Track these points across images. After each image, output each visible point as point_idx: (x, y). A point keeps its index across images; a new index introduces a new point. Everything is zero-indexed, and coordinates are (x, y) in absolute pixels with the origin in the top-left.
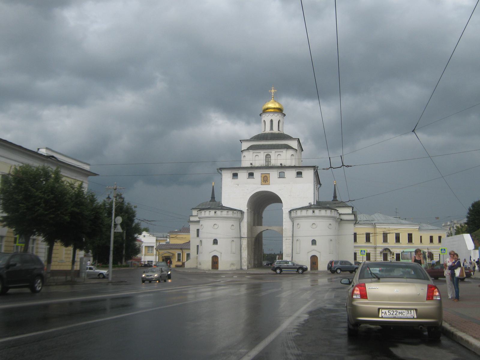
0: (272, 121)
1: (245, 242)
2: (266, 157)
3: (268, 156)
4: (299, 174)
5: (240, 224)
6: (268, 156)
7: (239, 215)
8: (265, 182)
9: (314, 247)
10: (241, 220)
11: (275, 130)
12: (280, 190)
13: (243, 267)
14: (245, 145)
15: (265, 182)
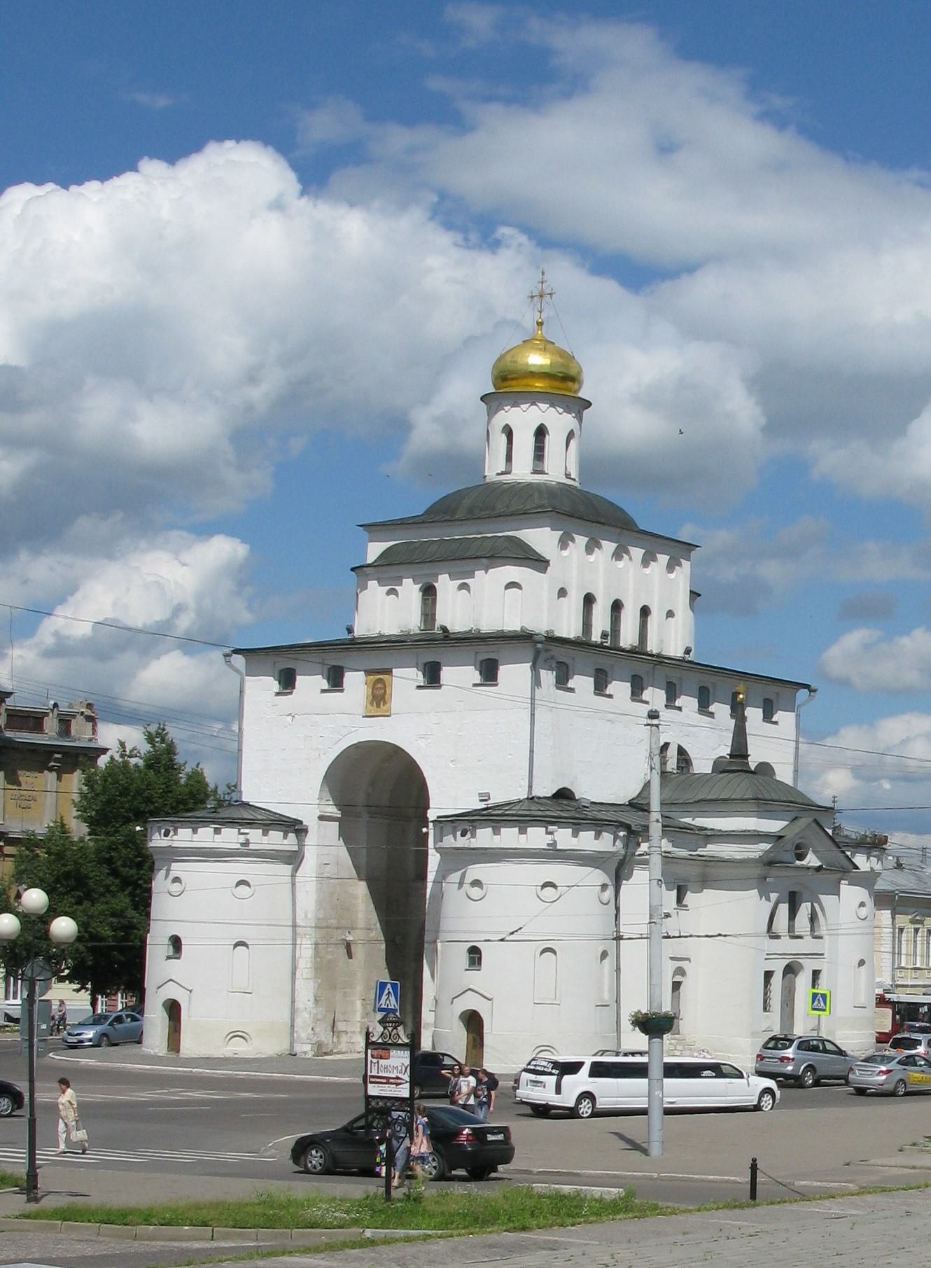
0: (509, 432)
1: (306, 953)
2: (424, 601)
3: (429, 592)
4: (489, 673)
5: (293, 876)
6: (429, 592)
7: (276, 840)
8: (378, 706)
9: (474, 979)
10: (294, 859)
11: (522, 471)
12: (423, 737)
13: (299, 1048)
14: (375, 550)
15: (378, 706)
